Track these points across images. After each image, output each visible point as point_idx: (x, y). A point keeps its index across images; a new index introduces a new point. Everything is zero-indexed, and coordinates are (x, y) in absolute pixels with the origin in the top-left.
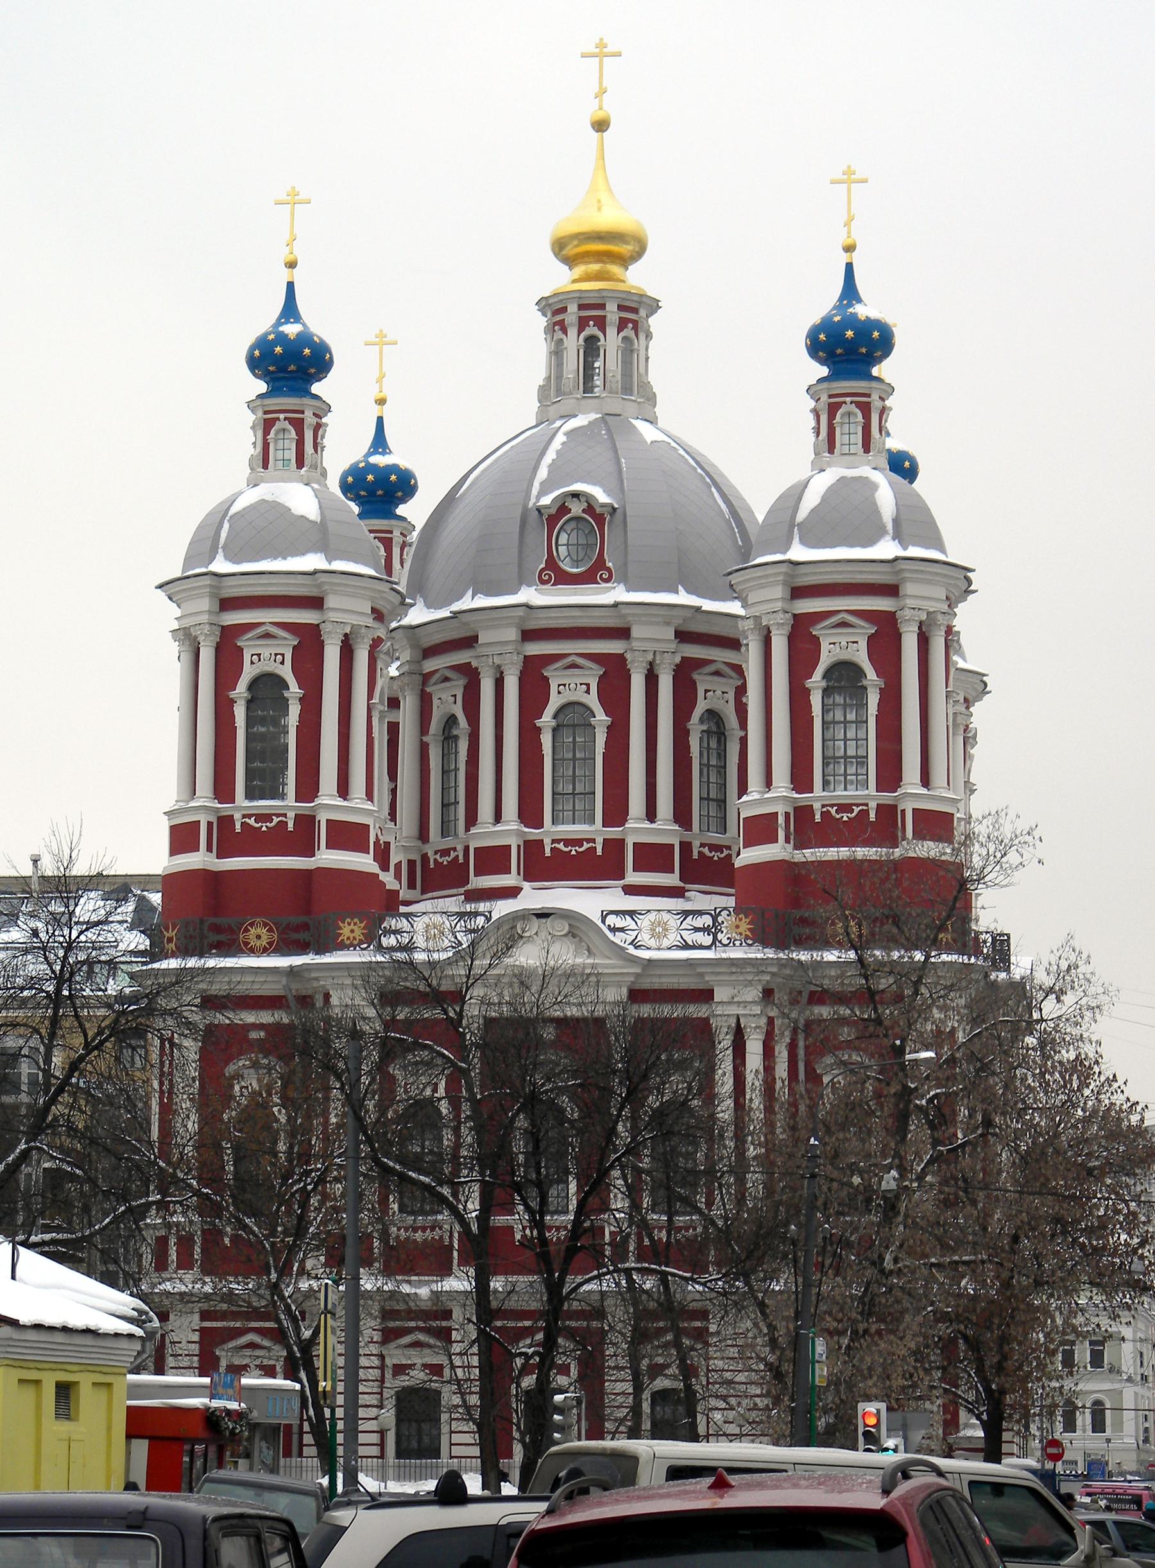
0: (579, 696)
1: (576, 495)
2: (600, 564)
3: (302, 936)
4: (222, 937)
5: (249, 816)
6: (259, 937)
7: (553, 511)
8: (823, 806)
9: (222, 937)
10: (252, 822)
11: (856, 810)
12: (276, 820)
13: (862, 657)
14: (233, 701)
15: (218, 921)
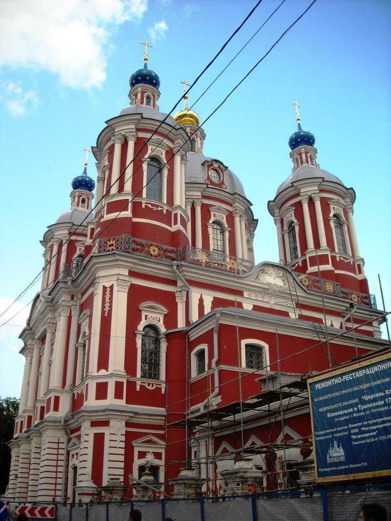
0: (219, 219)
1: (216, 161)
2: (223, 183)
3: (174, 255)
4: (138, 247)
5: (149, 204)
6: (154, 251)
7: (210, 163)
8: (340, 257)
9: (138, 247)
10: (150, 206)
11: (349, 261)
12: (160, 209)
13: (342, 214)
14: (142, 162)
15: (136, 239)
